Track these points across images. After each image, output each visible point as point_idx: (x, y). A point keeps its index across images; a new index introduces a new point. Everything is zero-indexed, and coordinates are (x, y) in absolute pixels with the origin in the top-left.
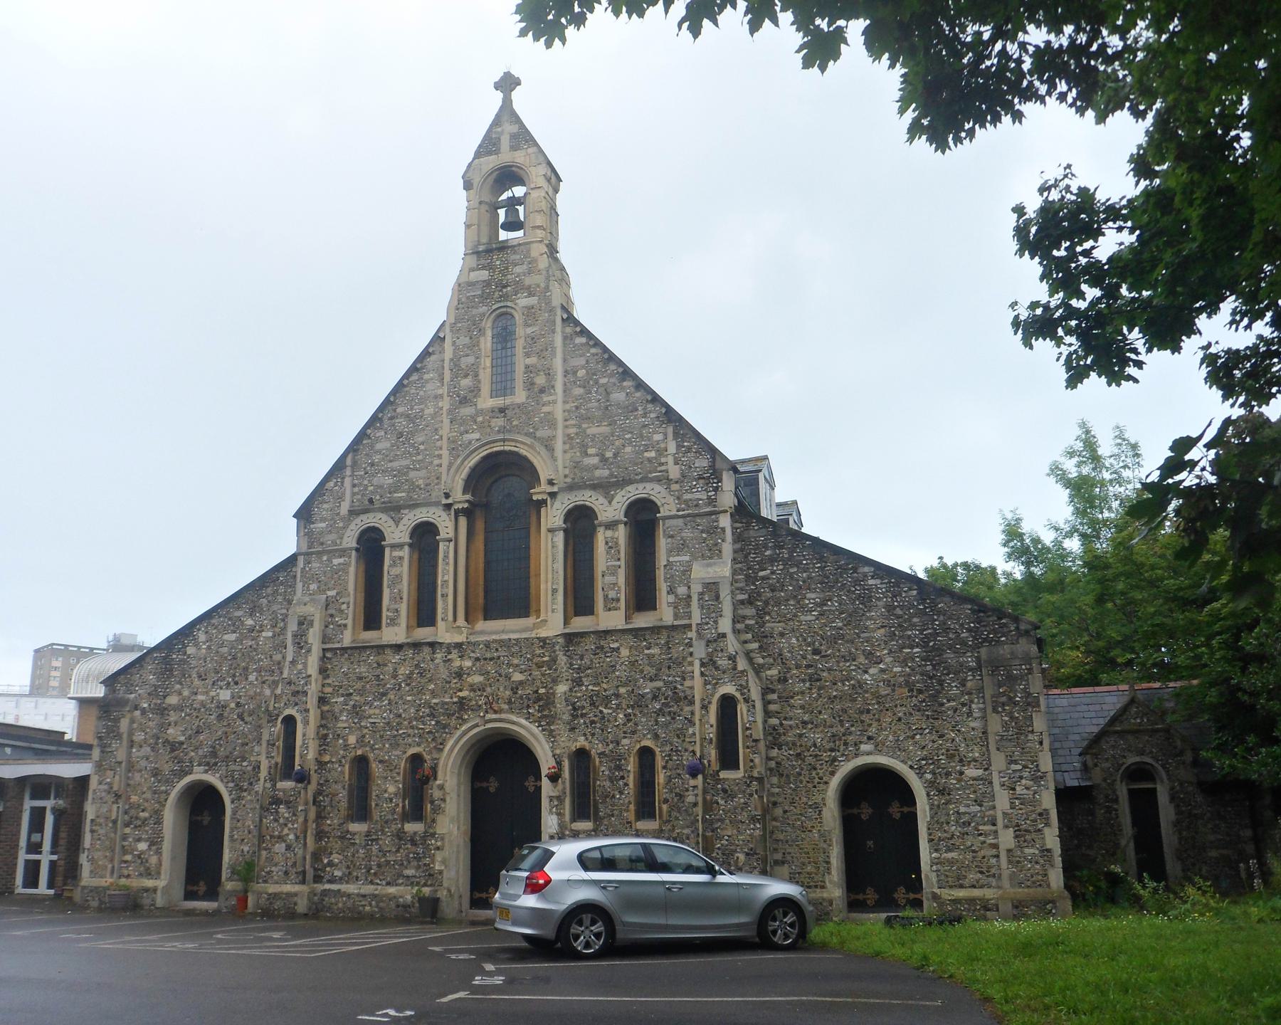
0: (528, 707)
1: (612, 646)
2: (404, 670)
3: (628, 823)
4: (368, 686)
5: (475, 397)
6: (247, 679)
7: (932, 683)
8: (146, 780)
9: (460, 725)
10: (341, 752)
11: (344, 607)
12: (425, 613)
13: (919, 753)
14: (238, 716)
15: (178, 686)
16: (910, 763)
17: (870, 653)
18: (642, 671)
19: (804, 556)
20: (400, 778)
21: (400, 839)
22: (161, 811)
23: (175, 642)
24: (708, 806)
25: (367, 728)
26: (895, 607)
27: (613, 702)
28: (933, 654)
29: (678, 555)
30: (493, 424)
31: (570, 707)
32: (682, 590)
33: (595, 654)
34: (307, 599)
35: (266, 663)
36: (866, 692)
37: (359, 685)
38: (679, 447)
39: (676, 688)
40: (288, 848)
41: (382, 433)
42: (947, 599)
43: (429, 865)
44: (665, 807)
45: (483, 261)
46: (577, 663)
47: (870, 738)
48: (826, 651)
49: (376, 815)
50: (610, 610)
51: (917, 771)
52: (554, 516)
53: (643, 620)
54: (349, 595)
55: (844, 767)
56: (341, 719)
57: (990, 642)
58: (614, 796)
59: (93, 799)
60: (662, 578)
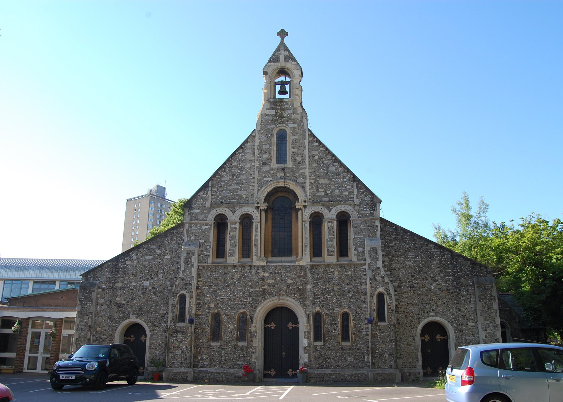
0: (294, 294)
1: (331, 270)
2: (237, 276)
3: (338, 342)
4: (220, 283)
6: (158, 277)
7: (456, 290)
8: (105, 320)
9: (263, 300)
10: (207, 311)
11: (208, 247)
12: (246, 251)
13: (452, 316)
14: (153, 293)
15: (122, 279)
16: (448, 320)
17: (433, 278)
18: (344, 281)
19: (407, 239)
20: (236, 322)
21: (235, 348)
23: (120, 258)
24: (373, 336)
26: (442, 261)
27: (332, 293)
28: (457, 279)
29: (359, 235)
30: (278, 175)
31: (313, 295)
32: (360, 249)
33: (324, 273)
34: (190, 243)
35: (167, 270)
36: (432, 292)
37: (215, 282)
38: (358, 192)
39: (358, 288)
40: (182, 352)
41: (226, 174)
42: (462, 259)
43: (249, 359)
44: (354, 336)
45: (272, 106)
47: (433, 310)
48: (416, 276)
49: (224, 339)
50: (330, 255)
51: (451, 323)
52: (305, 216)
53: (344, 261)
54: (210, 242)
55: (423, 321)
57: (477, 276)
58: (332, 331)
60: (352, 244)
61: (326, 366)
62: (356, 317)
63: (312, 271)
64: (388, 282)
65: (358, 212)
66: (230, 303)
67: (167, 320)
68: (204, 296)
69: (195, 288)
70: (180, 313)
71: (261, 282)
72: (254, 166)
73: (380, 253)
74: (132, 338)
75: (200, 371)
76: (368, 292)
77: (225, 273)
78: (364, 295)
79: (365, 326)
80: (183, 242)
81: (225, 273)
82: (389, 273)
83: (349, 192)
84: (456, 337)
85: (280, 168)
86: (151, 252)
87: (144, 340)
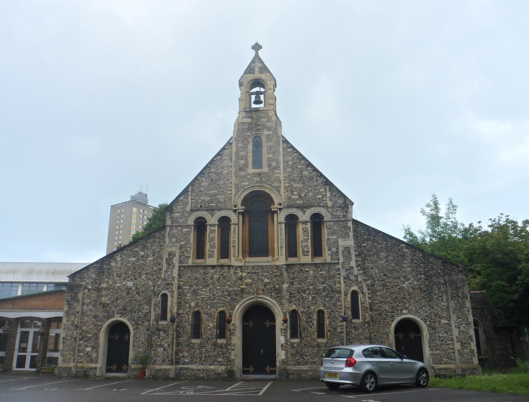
0: (271, 293)
2: (216, 276)
4: (200, 282)
5: (246, 168)
6: (141, 277)
7: (429, 288)
8: (90, 320)
9: (242, 299)
12: (224, 253)
14: (137, 293)
15: (107, 280)
16: (421, 318)
17: (405, 276)
18: (318, 280)
19: (379, 239)
20: (215, 320)
21: (215, 346)
22: (98, 334)
23: (105, 260)
24: (348, 334)
25: (199, 299)
28: (428, 278)
29: (332, 236)
30: (254, 180)
31: (289, 293)
32: (334, 249)
33: (299, 273)
34: (171, 245)
35: (150, 271)
36: (404, 291)
37: (196, 282)
38: (331, 194)
39: (332, 287)
40: (164, 350)
41: (204, 179)
42: (433, 258)
43: (228, 356)
44: (329, 333)
45: (248, 115)
46: (292, 276)
47: (406, 308)
49: (204, 336)
50: (305, 255)
53: (318, 260)
54: (191, 244)
56: (188, 295)
57: (449, 274)
58: (308, 329)
59: (64, 328)
61: (303, 362)
62: (331, 315)
63: (288, 271)
64: (361, 281)
65: (331, 214)
66: (209, 302)
67: (150, 318)
68: (185, 295)
69: (177, 287)
70: (162, 311)
71: (239, 281)
72: (231, 171)
73: (353, 253)
74: (117, 337)
75: (181, 368)
76: (343, 291)
77: (205, 274)
78: (338, 293)
79: (340, 324)
80: (165, 244)
81: (205, 274)
82: (362, 272)
83: (322, 195)
84: (430, 334)
85: (256, 173)
86: (134, 254)
87: (128, 339)
